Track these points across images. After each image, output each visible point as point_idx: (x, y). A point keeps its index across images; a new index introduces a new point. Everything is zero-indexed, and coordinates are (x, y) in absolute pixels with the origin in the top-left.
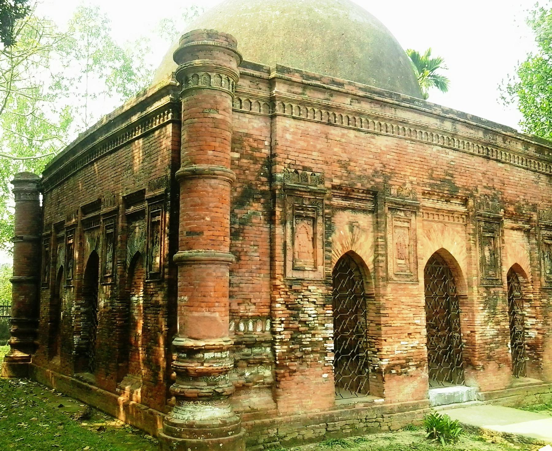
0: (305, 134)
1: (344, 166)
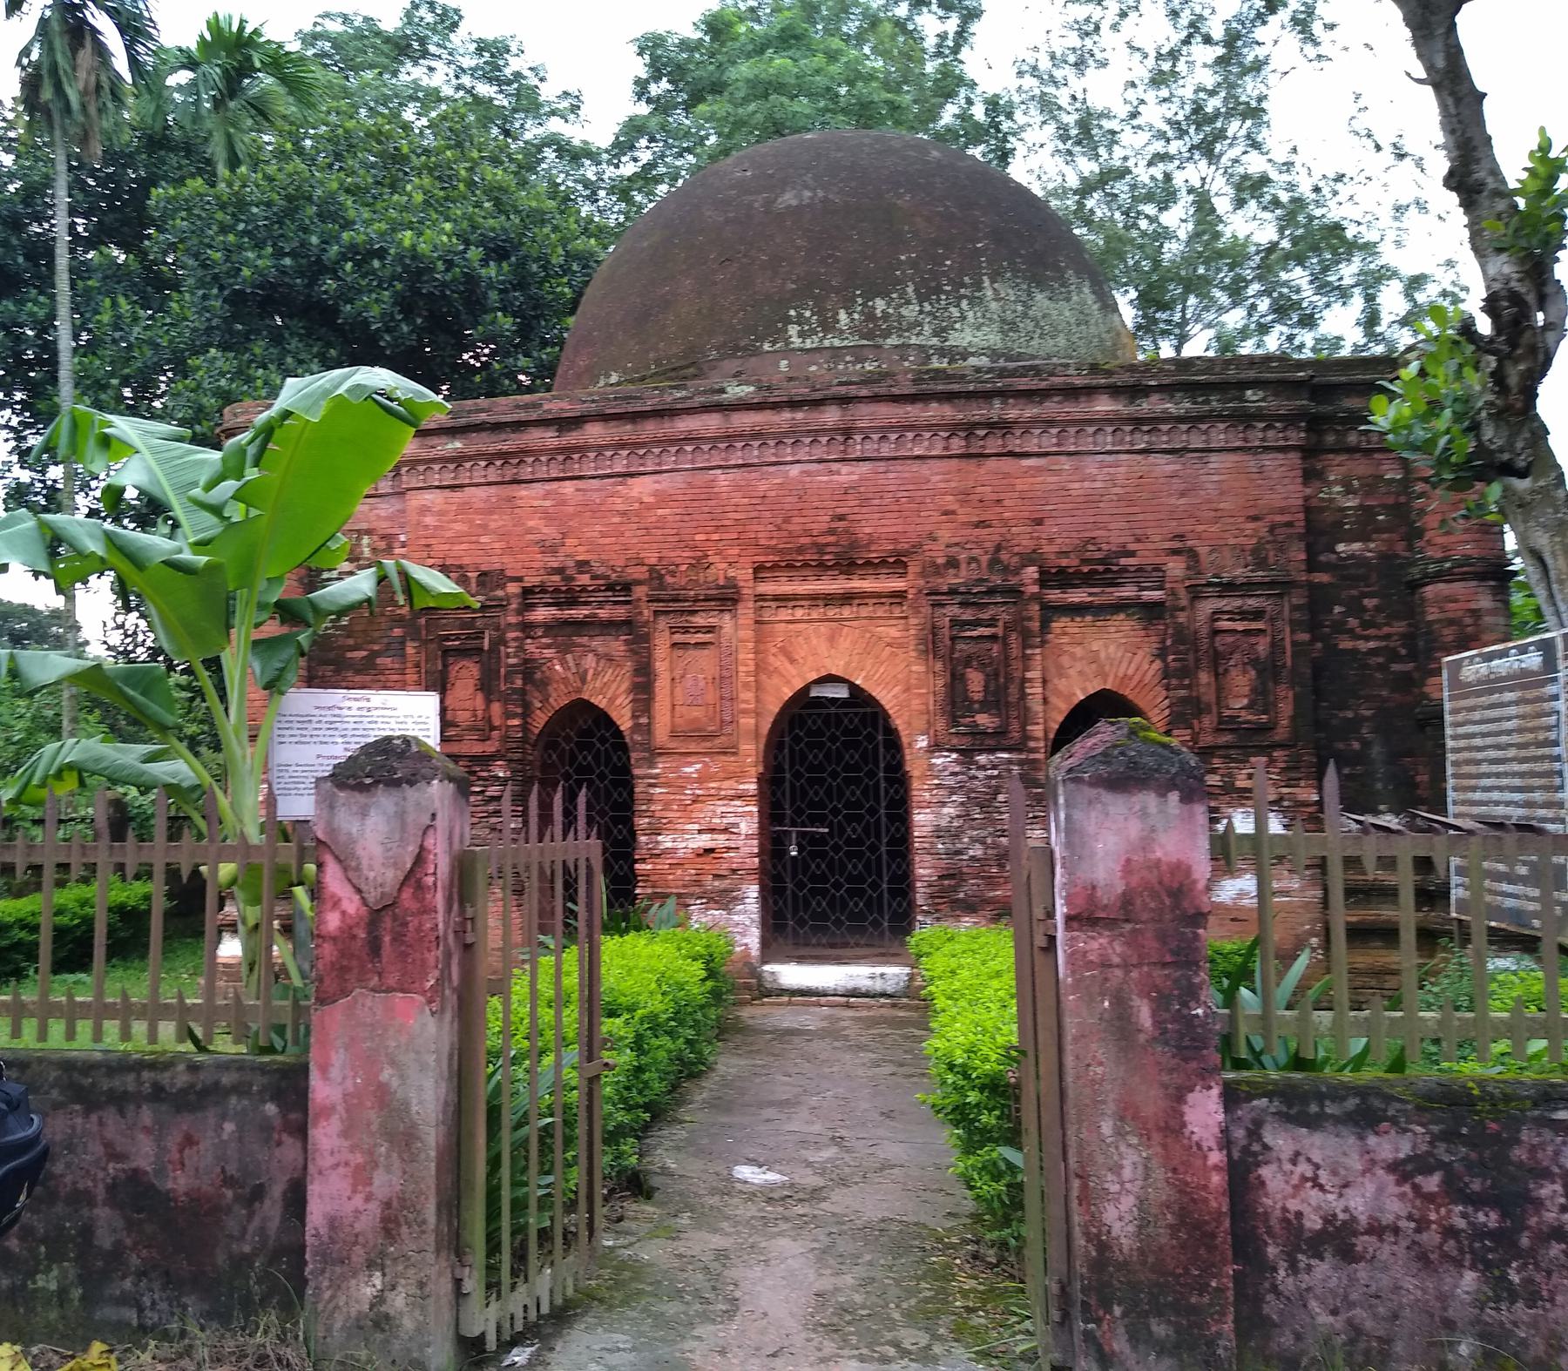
0: (465, 508)
1: (550, 549)
